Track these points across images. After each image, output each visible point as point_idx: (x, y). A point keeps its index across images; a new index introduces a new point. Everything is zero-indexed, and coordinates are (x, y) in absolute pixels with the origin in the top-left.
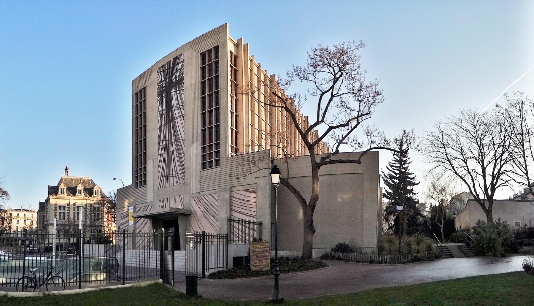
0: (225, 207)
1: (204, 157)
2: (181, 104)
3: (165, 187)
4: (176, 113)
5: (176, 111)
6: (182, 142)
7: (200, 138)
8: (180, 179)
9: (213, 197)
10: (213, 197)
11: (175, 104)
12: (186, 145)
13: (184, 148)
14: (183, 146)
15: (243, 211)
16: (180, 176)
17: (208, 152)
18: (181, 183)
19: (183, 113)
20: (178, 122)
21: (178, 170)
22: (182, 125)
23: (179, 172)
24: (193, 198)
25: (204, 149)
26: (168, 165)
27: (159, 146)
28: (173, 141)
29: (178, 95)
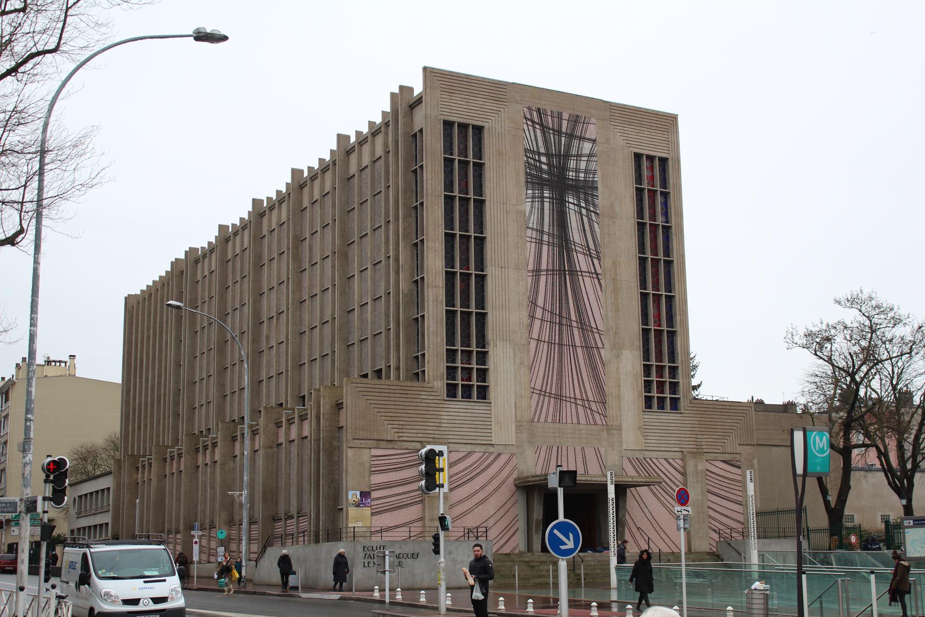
0: (699, 484)
1: (648, 385)
2: (592, 246)
3: (554, 422)
4: (582, 262)
5: (581, 257)
6: (597, 336)
7: (639, 343)
8: (597, 416)
9: (670, 464)
10: (670, 464)
11: (575, 235)
12: (607, 345)
13: (602, 351)
14: (600, 345)
15: (722, 493)
16: (594, 408)
17: (654, 378)
18: (599, 422)
19: (599, 271)
20: (587, 284)
21: (589, 393)
22: (598, 299)
23: (591, 398)
24: (629, 459)
25: (647, 369)
26: (560, 372)
27: (532, 317)
28: (574, 324)
29: (585, 219)
